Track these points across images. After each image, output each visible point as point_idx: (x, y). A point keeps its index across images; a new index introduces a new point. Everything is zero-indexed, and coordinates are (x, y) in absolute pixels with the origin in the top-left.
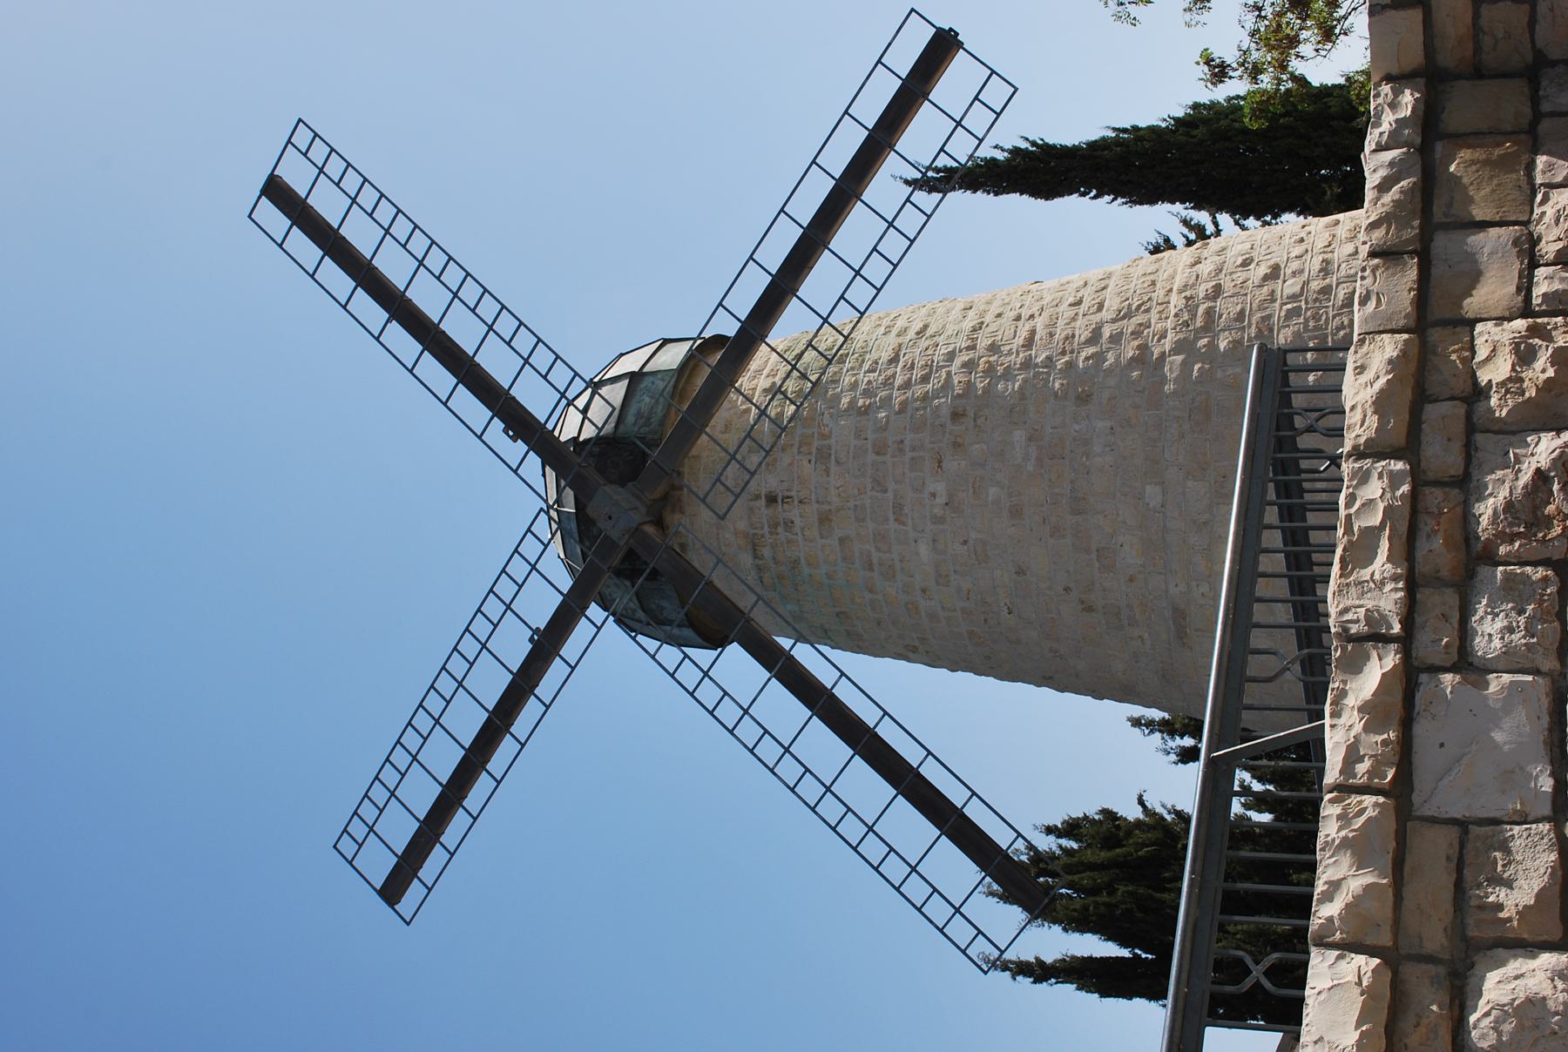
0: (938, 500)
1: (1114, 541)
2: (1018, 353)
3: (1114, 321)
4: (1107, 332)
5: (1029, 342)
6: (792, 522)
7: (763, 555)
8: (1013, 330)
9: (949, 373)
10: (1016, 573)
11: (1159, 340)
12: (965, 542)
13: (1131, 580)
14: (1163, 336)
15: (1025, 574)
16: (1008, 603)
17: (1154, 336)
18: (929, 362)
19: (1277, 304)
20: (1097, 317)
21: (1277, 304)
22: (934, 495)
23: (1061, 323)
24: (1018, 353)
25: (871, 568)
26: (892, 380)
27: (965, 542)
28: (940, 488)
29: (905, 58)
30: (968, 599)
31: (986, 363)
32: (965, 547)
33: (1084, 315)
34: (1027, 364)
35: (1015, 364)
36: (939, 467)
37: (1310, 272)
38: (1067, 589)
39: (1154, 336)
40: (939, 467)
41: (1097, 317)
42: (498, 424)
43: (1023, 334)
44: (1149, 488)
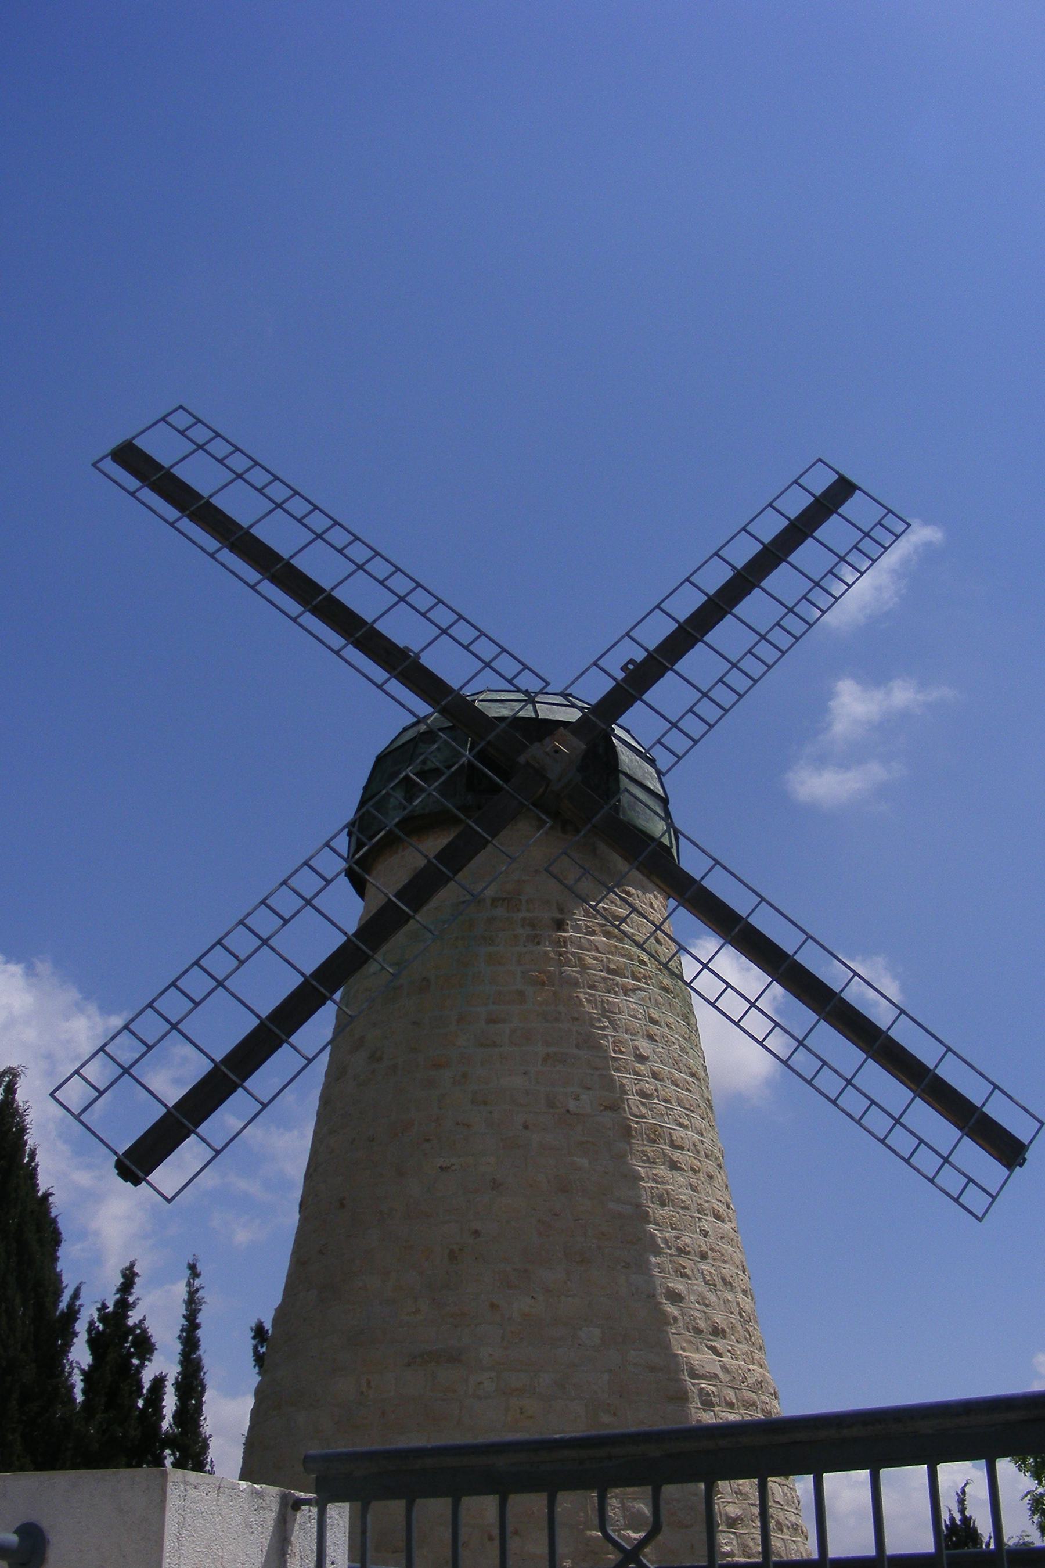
1: (537, 1289)
2: (707, 1202)
6: (538, 944)
7: (496, 907)
8: (721, 1199)
9: (685, 1127)
10: (494, 1179)
11: (729, 1351)
13: (493, 1306)
15: (493, 1189)
16: (454, 1168)
17: (731, 1346)
18: (692, 1108)
22: (577, 1098)
24: (707, 1202)
25: (491, 1021)
26: (676, 1067)
27: (526, 1127)
29: (999, 1111)
30: (458, 1124)
31: (699, 1168)
32: (521, 1127)
33: (737, 1274)
35: (700, 1198)
36: (606, 1108)
37: (788, 1511)
38: (476, 1233)
39: (731, 1346)
40: (606, 1108)
42: (640, 655)
44: (597, 1332)
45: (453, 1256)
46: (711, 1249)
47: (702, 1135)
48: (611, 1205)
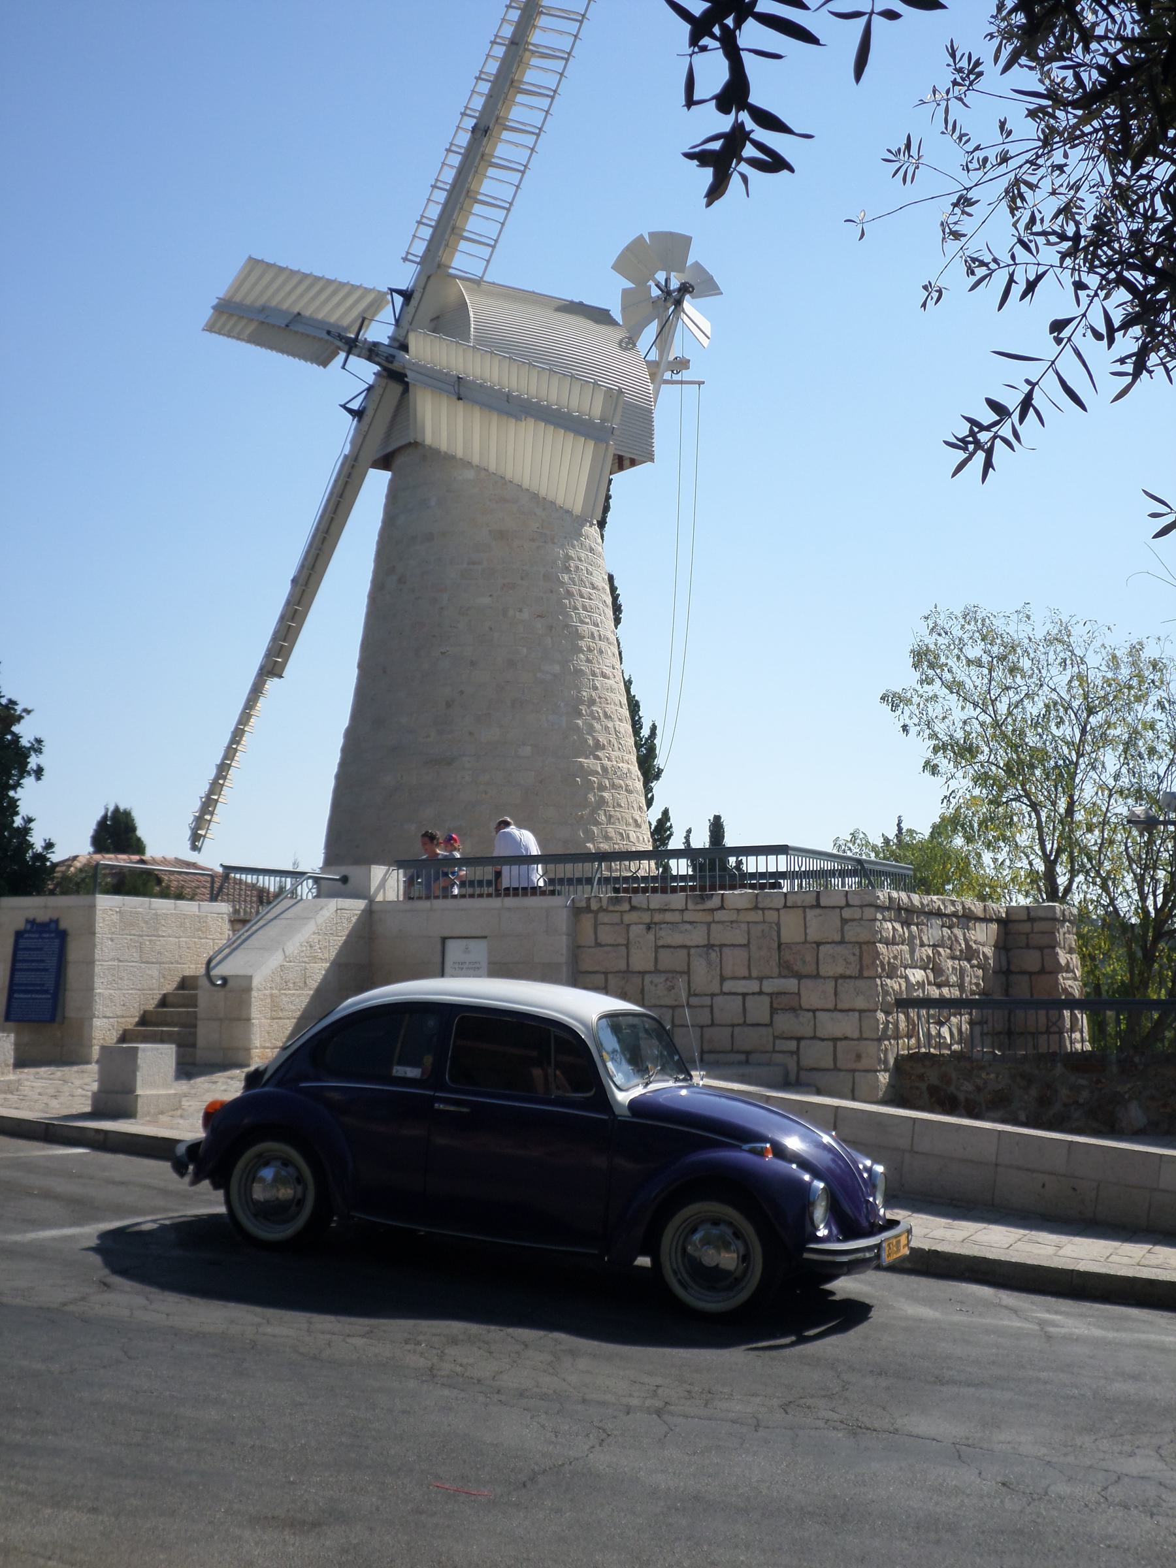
0: (518, 613)
3: (615, 728)
4: (610, 725)
5: (604, 676)
9: (587, 624)
12: (491, 629)
14: (609, 759)
19: (625, 827)
20: (616, 719)
21: (625, 827)
22: (521, 611)
23: (612, 695)
27: (491, 629)
28: (525, 615)
34: (594, 674)
38: (462, 692)
41: (616, 719)
43: (608, 671)
45: (448, 705)
46: (600, 697)
47: (598, 626)
48: (539, 675)
